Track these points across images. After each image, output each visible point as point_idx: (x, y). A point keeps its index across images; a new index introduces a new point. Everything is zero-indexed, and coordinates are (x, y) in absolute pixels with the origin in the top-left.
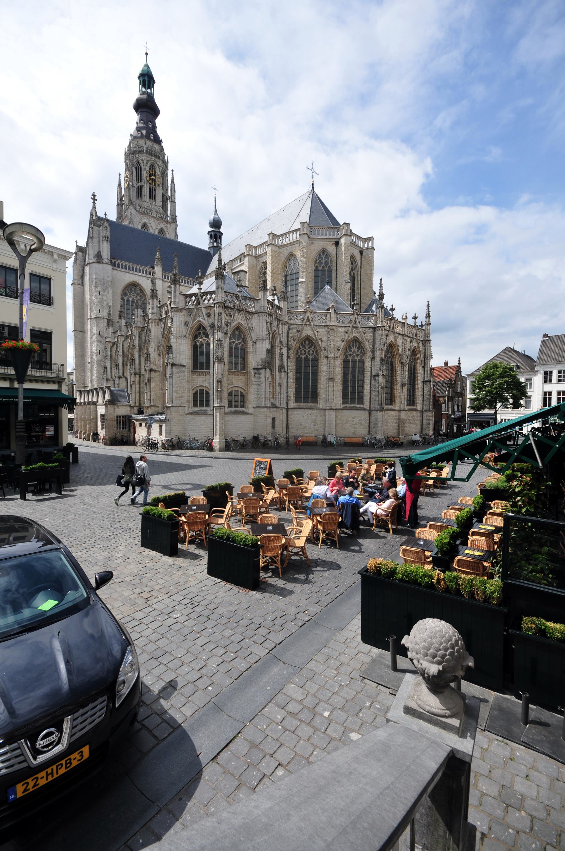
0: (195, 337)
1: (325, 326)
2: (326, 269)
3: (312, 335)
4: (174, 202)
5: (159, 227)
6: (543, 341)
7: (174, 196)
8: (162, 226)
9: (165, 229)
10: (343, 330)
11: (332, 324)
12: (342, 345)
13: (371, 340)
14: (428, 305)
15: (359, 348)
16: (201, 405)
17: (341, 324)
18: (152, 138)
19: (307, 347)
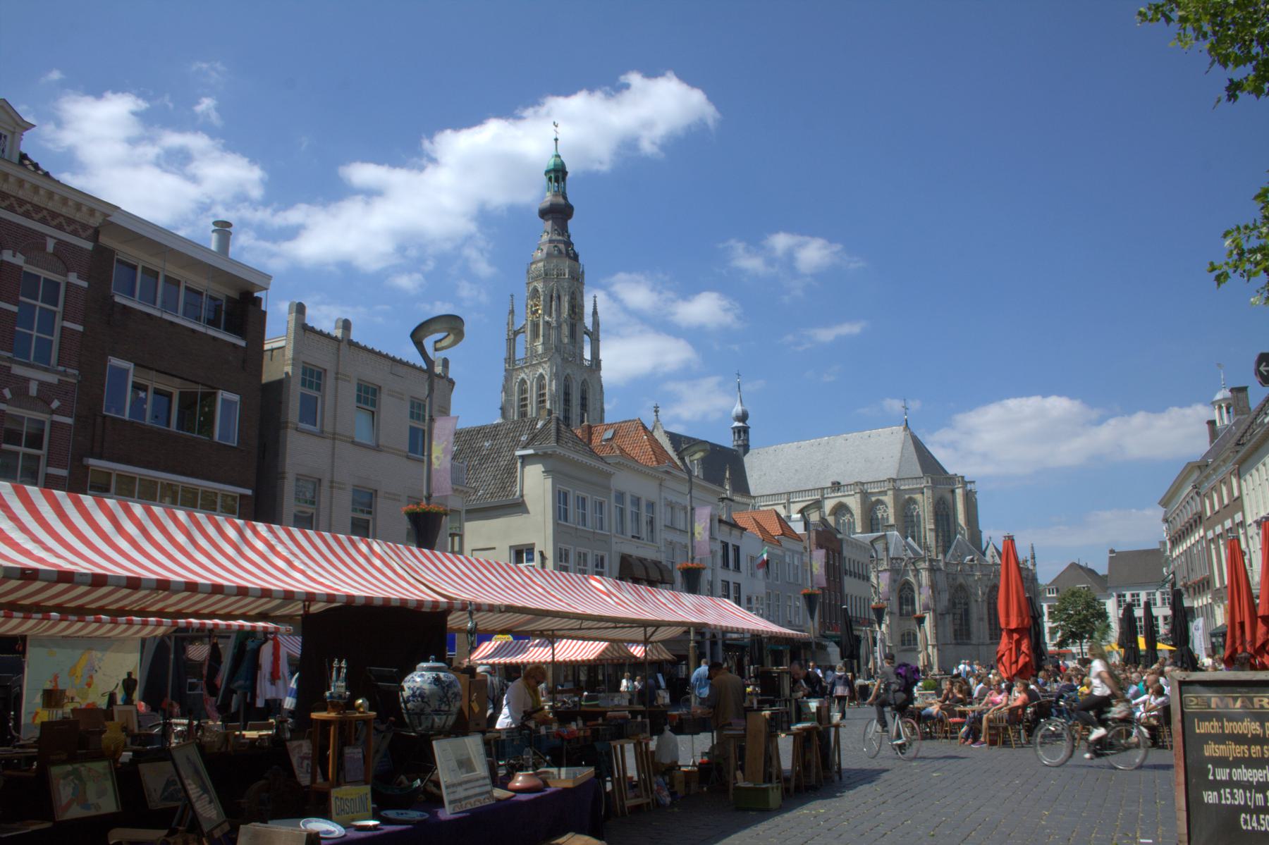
0: (901, 591)
2: (944, 513)
5: (583, 378)
6: (1111, 558)
7: (598, 332)
8: (585, 376)
12: (987, 590)
14: (1032, 548)
16: (909, 644)
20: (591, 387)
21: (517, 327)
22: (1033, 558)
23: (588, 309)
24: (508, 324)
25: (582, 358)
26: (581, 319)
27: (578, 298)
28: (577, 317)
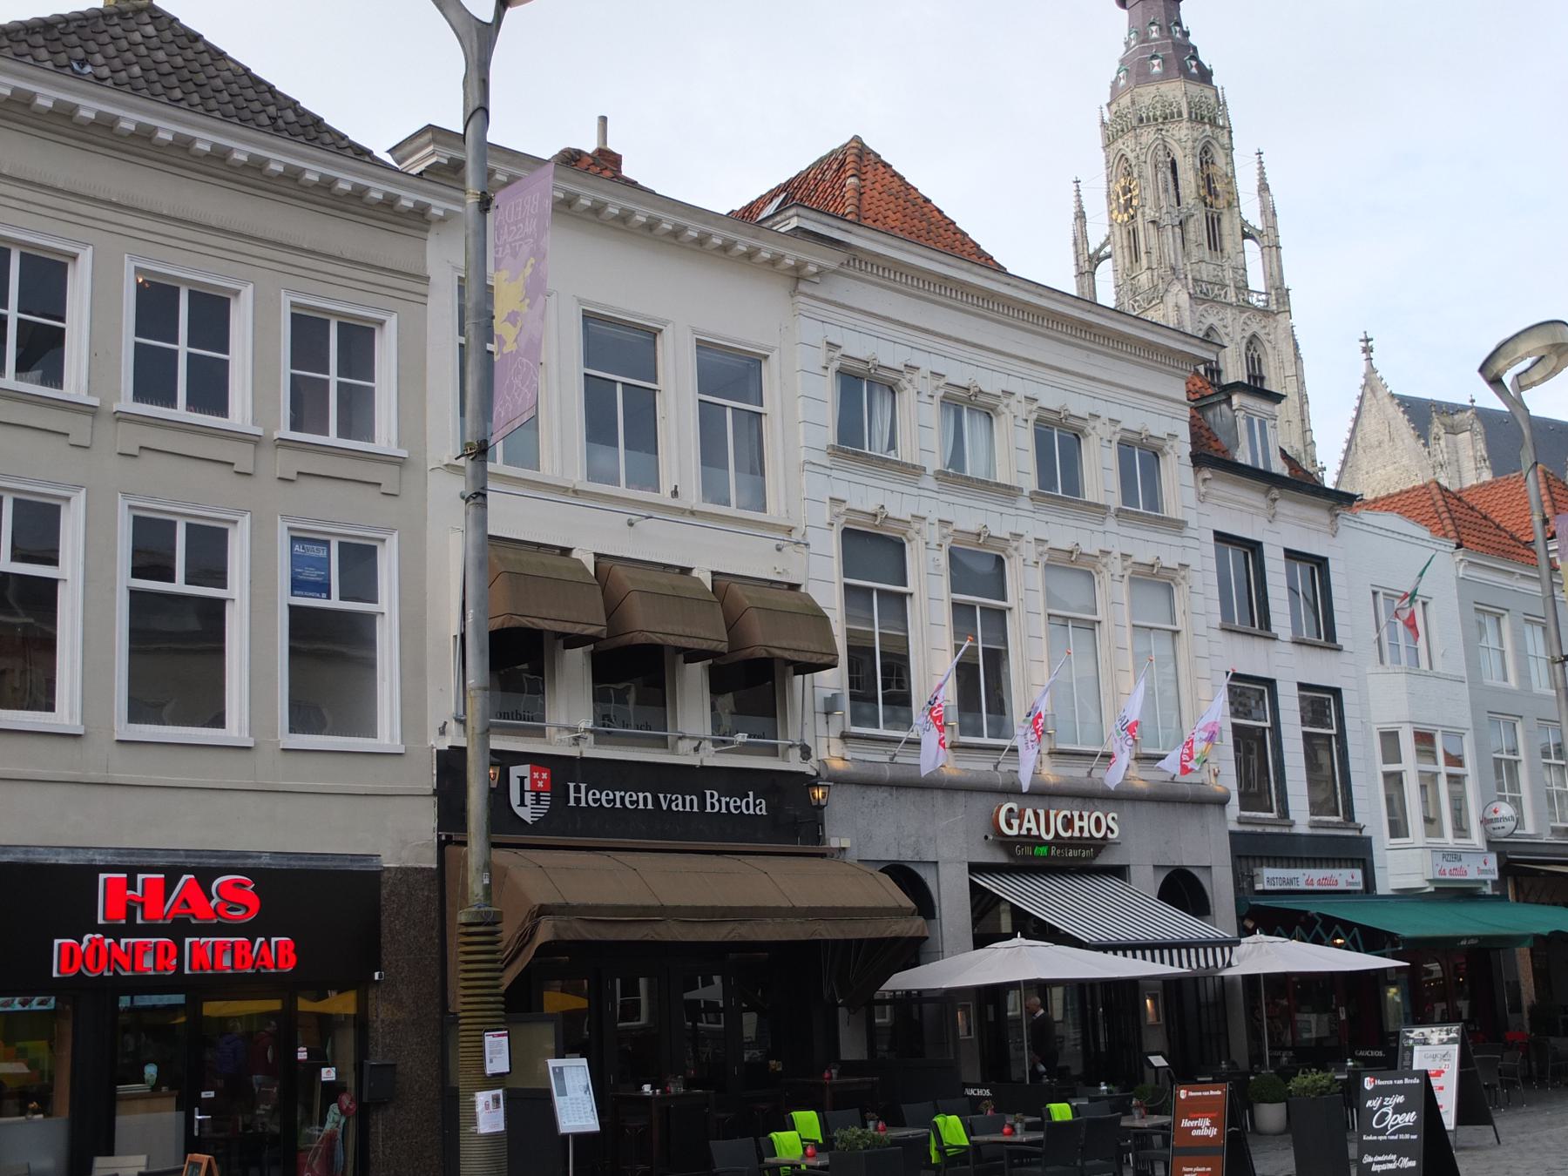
4: (1278, 248)
5: (1248, 334)
7: (1275, 228)
8: (1255, 327)
9: (1261, 334)
18: (1194, 70)
20: (1269, 350)
21: (1094, 245)
23: (1246, 185)
24: (1075, 244)
25: (1243, 287)
26: (1233, 203)
27: (1220, 160)
28: (1221, 203)
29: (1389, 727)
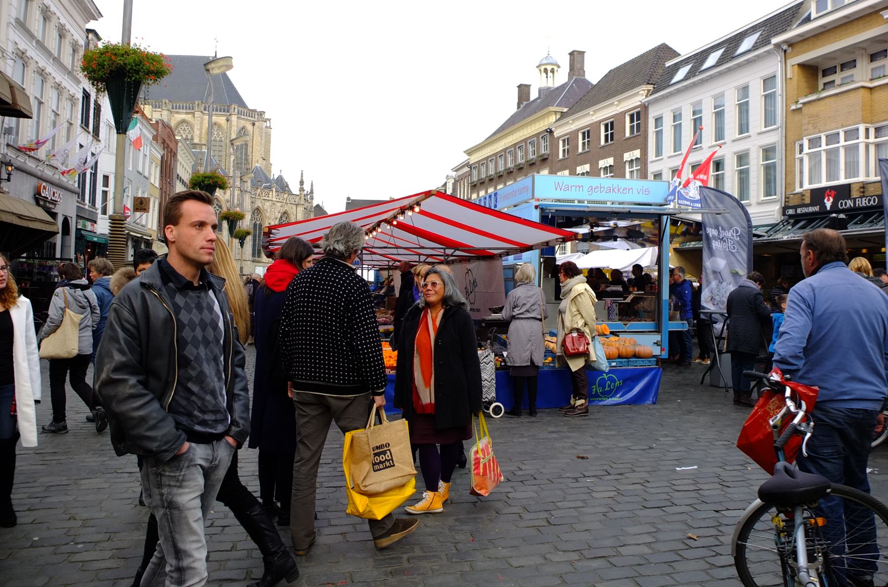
1: (269, 200)
3: (261, 207)
6: (347, 203)
10: (279, 204)
11: (274, 199)
12: (279, 215)
13: (295, 213)
15: (287, 218)
17: (278, 200)
19: (256, 215)
22: (312, 192)
29: (106, 174)
